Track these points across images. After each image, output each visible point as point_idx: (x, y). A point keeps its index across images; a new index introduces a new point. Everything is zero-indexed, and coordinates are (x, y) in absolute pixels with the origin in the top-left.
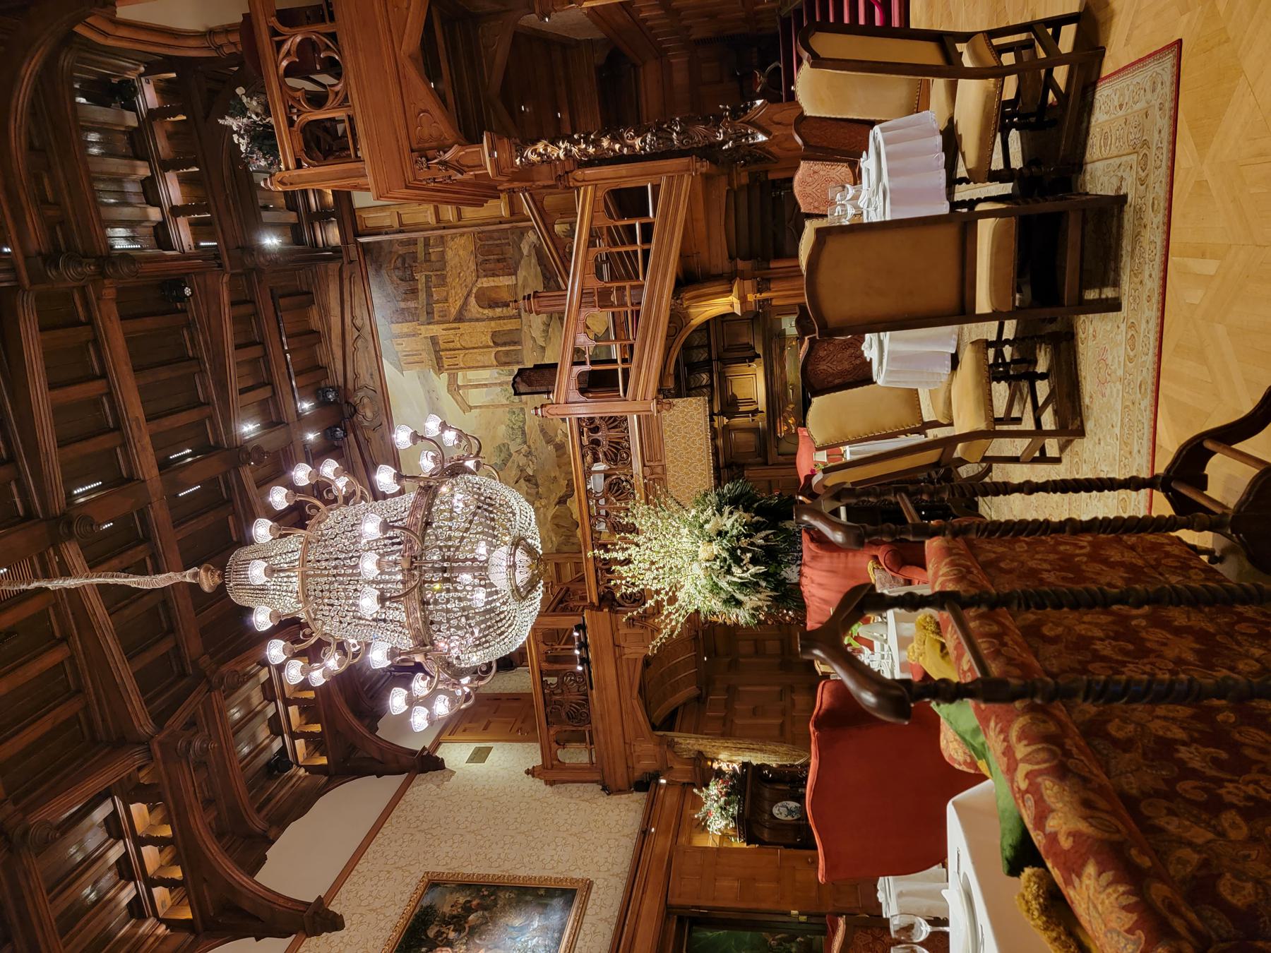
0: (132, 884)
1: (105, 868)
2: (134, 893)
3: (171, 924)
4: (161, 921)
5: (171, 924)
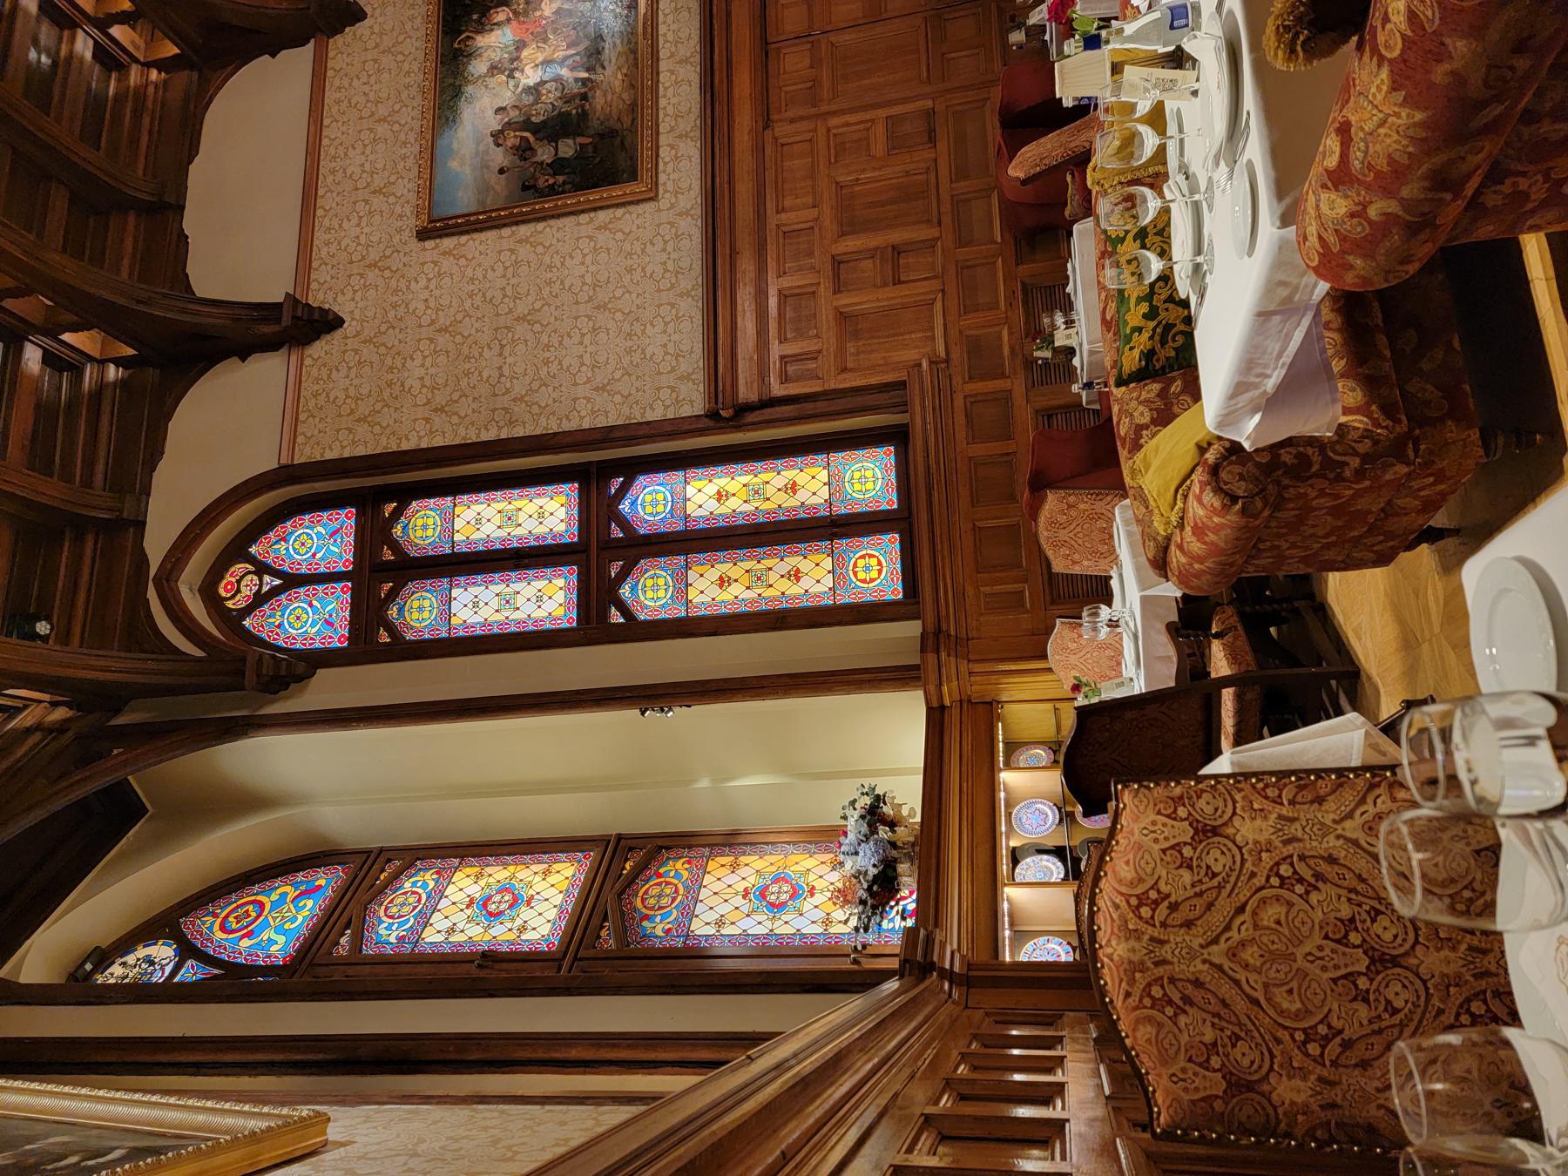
0: (80, 31)
1: (33, 22)
2: (91, 43)
3: (161, 65)
4: (148, 65)
5: (161, 65)
